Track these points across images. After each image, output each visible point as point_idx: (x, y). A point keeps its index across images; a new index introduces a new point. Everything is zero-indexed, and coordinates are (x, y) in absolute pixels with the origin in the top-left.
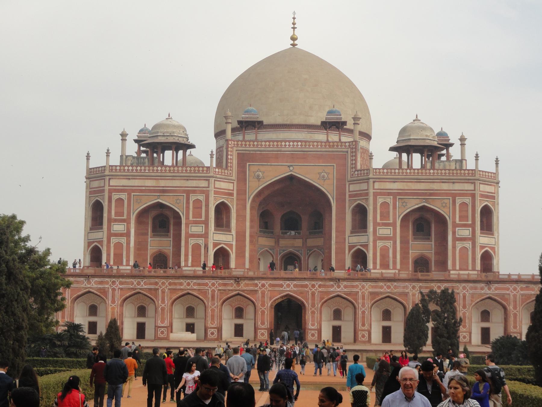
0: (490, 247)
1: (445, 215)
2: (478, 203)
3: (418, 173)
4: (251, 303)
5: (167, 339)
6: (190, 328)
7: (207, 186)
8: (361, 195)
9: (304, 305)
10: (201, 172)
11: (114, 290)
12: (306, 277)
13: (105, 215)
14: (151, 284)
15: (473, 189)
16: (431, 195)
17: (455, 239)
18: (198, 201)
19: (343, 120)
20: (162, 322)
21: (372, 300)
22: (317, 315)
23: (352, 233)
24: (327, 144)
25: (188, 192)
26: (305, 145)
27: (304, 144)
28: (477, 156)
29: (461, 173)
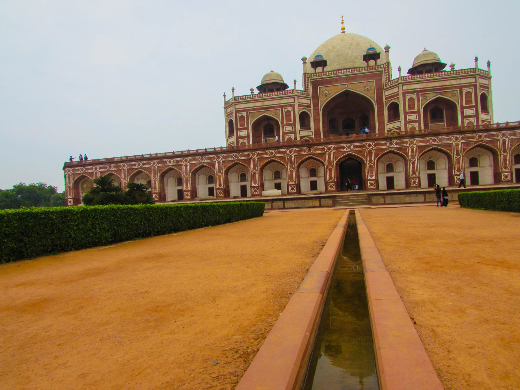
0: (488, 121)
2: (478, 91)
3: (433, 76)
4: (321, 164)
5: (260, 195)
6: (278, 186)
8: (394, 96)
9: (363, 162)
11: (219, 163)
14: (245, 156)
16: (444, 89)
17: (463, 117)
18: (288, 112)
20: (255, 183)
21: (420, 152)
23: (389, 122)
25: (282, 107)
28: (476, 59)
29: (465, 72)
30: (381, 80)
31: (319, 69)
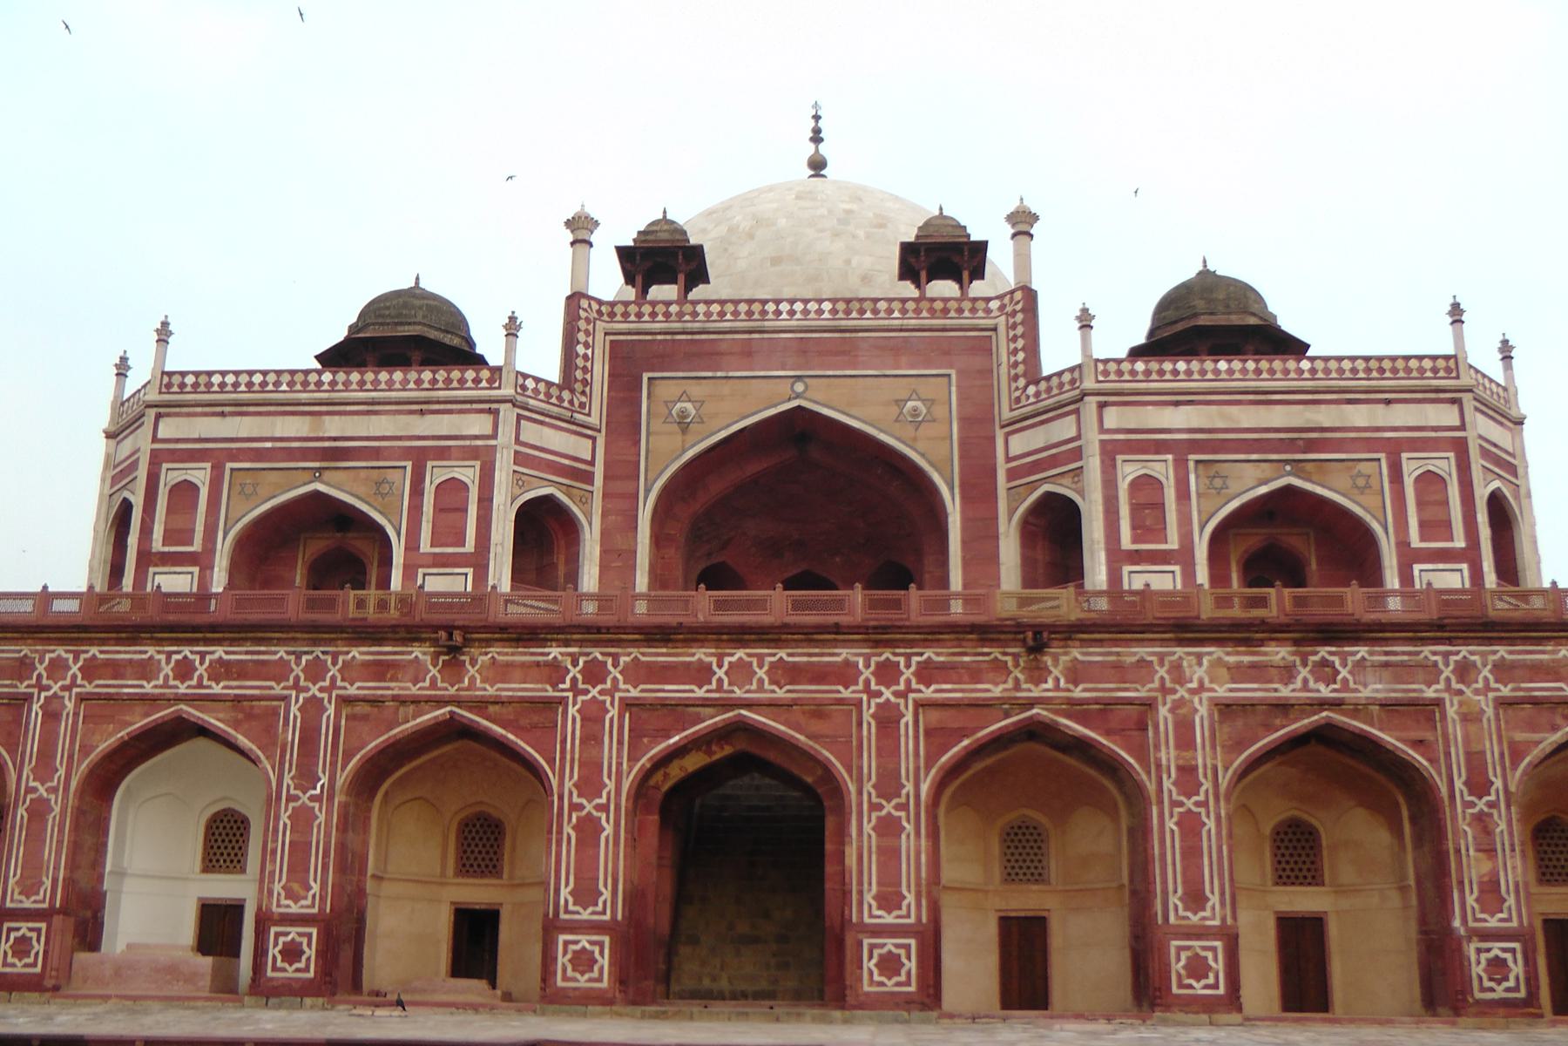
1: (1368, 518)
3: (1258, 371)
7: (488, 431)
8: (1054, 461)
9: (838, 791)
10: (469, 384)
12: (844, 619)
13: (133, 540)
15: (1457, 423)
16: (1311, 446)
19: (973, 238)
22: (907, 842)
24: (925, 305)
25: (420, 457)
26: (848, 312)
27: (841, 306)
30: (987, 372)
31: (663, 292)
